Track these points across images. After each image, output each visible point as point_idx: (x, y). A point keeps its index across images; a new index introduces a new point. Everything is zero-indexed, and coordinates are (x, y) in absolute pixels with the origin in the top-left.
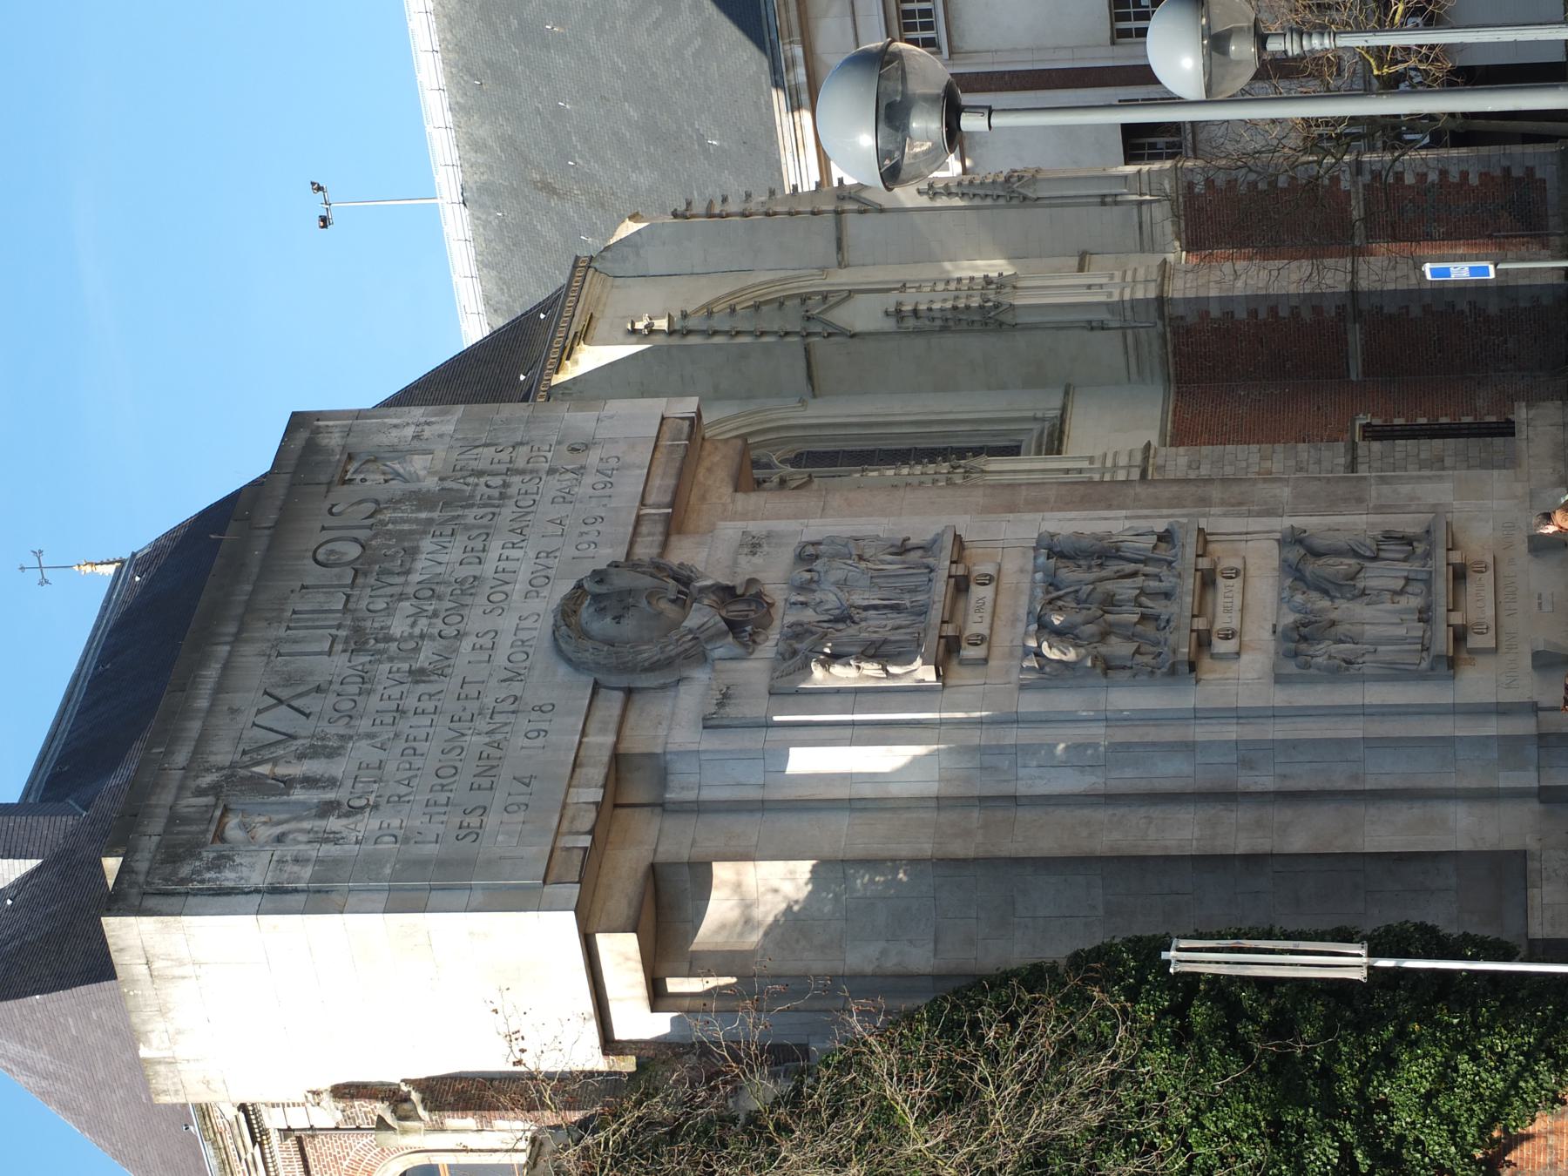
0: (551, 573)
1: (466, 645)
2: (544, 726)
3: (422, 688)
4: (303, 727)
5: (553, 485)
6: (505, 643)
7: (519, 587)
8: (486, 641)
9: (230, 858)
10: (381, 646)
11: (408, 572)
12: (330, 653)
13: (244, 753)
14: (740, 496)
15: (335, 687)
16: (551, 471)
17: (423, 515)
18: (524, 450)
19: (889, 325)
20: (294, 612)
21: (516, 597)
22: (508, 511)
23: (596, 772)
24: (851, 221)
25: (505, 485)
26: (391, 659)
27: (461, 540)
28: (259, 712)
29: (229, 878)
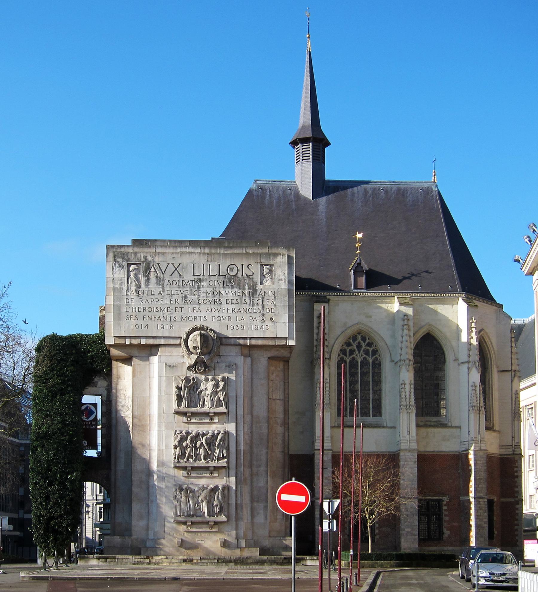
0: (222, 320)
1: (197, 306)
2: (165, 328)
3: (180, 299)
4: (167, 276)
5: (258, 315)
6: (193, 315)
7: (217, 314)
8: (197, 310)
9: (123, 268)
10: (196, 287)
11: (224, 287)
12: (194, 275)
13: (158, 264)
14: (267, 359)
15: (182, 279)
16: (263, 315)
17: (247, 287)
18: (273, 306)
19: (401, 382)
20: (210, 265)
21: (213, 314)
22: (248, 307)
23: (151, 342)
24: (466, 366)
25: (258, 304)
26: (191, 290)
27: (235, 297)
28: (173, 264)
29: (117, 269)
